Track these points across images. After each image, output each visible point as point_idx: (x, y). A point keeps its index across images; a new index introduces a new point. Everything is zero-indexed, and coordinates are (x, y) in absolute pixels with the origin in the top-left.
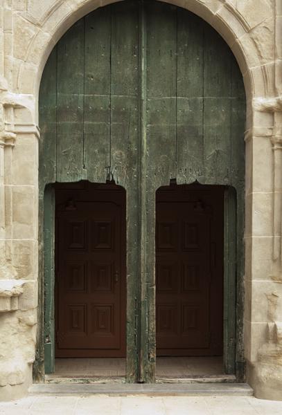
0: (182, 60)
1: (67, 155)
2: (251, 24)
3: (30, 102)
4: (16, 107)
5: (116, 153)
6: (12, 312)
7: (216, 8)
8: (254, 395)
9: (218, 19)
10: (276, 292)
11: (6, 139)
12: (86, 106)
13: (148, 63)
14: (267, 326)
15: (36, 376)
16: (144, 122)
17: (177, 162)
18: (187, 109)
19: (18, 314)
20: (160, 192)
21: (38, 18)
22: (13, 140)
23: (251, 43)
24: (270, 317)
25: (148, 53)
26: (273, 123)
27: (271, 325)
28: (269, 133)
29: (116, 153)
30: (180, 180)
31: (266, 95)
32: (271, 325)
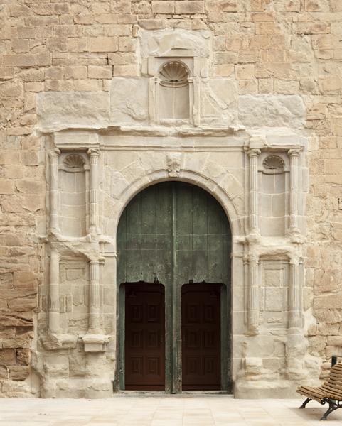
0: (195, 214)
1: (132, 267)
2: (231, 196)
3: (112, 240)
4: (105, 243)
5: (159, 266)
6: (103, 353)
7: (213, 188)
8: (234, 398)
9: (213, 193)
10: (246, 342)
11: (100, 260)
12: (142, 240)
13: (177, 217)
14: (242, 360)
15: (115, 390)
16: (175, 249)
17: (193, 270)
18: (199, 241)
19: (106, 353)
20: (184, 287)
21: (117, 195)
22: (104, 260)
23: (232, 206)
24: (243, 355)
25: (177, 210)
26: (244, 250)
27: (243, 359)
28: (242, 255)
29: (159, 266)
30: (195, 281)
31: (240, 234)
32: (243, 359)
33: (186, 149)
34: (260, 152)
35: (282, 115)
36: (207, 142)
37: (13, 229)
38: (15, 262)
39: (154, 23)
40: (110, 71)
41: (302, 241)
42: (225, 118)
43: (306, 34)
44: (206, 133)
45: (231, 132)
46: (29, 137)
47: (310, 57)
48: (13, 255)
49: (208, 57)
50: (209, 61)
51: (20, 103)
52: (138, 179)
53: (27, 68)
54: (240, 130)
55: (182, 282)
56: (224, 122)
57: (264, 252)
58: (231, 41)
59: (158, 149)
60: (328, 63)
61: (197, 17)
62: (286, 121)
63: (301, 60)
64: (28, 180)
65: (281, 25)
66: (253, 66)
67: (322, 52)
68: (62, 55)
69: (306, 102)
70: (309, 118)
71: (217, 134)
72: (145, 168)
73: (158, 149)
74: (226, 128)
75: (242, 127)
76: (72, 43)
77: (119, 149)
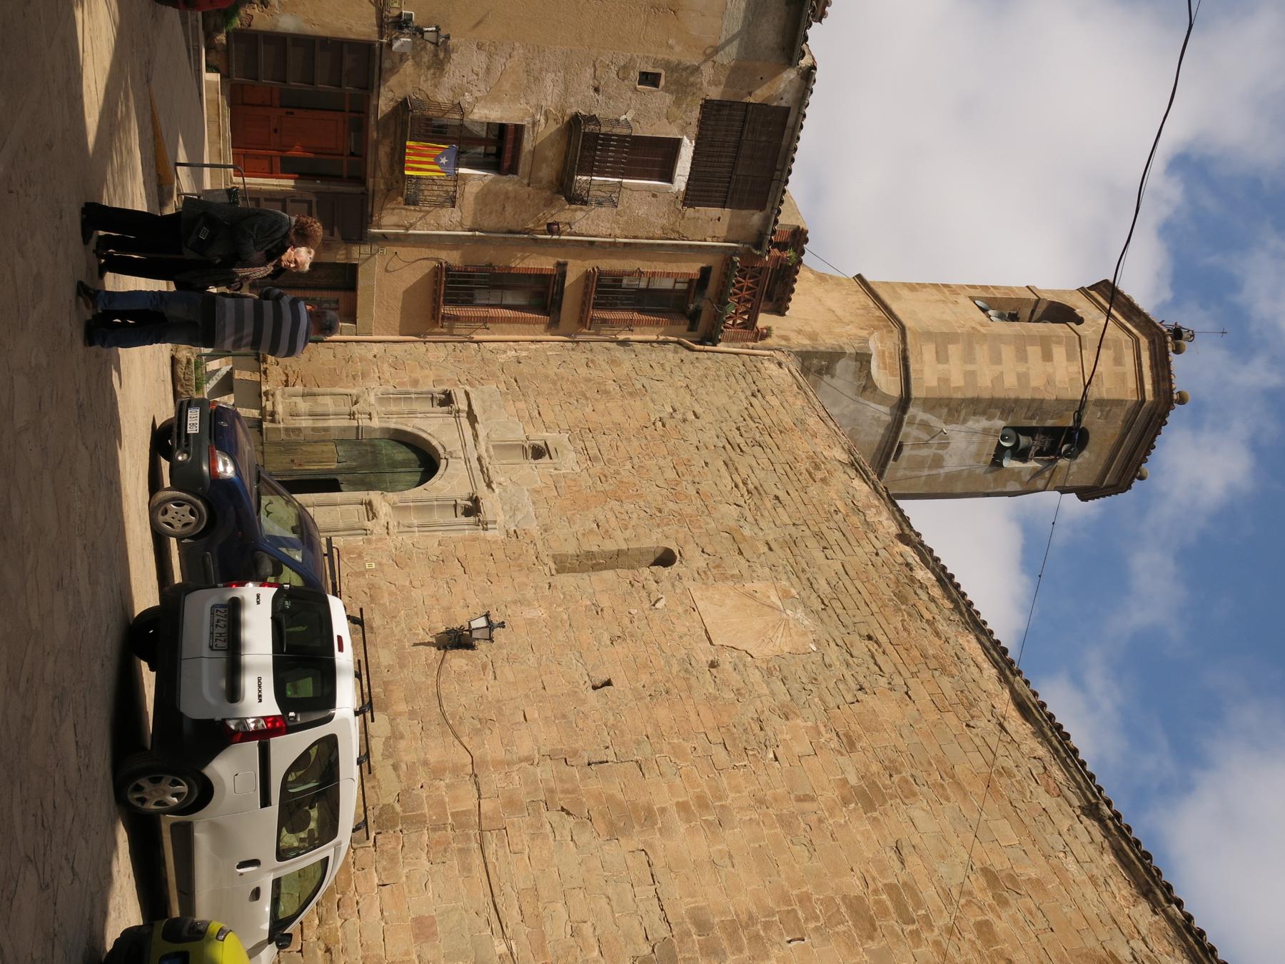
4: (370, 419)
33: (467, 461)
34: (474, 496)
35: (514, 513)
36: (477, 473)
37: (378, 375)
38: (347, 376)
39: (575, 439)
40: (526, 419)
41: (390, 531)
42: (502, 479)
43: (598, 525)
44: (485, 469)
45: (489, 485)
46: (458, 382)
47: (576, 527)
48: (353, 376)
49: (556, 469)
50: (552, 470)
51: (485, 377)
52: (433, 437)
53: (516, 381)
54: (493, 490)
55: (340, 478)
56: (496, 478)
57: (375, 503)
58: (575, 481)
59: (464, 446)
60: (575, 540)
61: (589, 462)
62: (510, 517)
63: (571, 522)
64: (421, 381)
65: (599, 508)
66: (556, 494)
67: (584, 534)
68: (532, 397)
69: (534, 528)
70: (517, 531)
71: (486, 477)
72: (444, 439)
73: (464, 446)
74: (492, 478)
75: (497, 491)
76: (540, 400)
77: (459, 426)
